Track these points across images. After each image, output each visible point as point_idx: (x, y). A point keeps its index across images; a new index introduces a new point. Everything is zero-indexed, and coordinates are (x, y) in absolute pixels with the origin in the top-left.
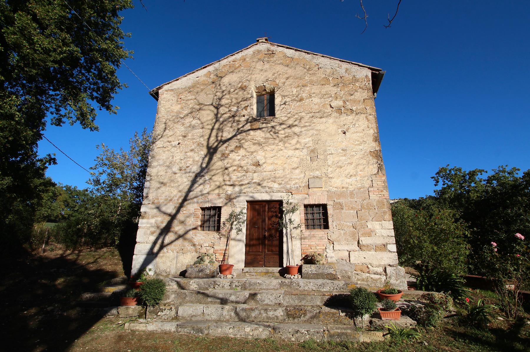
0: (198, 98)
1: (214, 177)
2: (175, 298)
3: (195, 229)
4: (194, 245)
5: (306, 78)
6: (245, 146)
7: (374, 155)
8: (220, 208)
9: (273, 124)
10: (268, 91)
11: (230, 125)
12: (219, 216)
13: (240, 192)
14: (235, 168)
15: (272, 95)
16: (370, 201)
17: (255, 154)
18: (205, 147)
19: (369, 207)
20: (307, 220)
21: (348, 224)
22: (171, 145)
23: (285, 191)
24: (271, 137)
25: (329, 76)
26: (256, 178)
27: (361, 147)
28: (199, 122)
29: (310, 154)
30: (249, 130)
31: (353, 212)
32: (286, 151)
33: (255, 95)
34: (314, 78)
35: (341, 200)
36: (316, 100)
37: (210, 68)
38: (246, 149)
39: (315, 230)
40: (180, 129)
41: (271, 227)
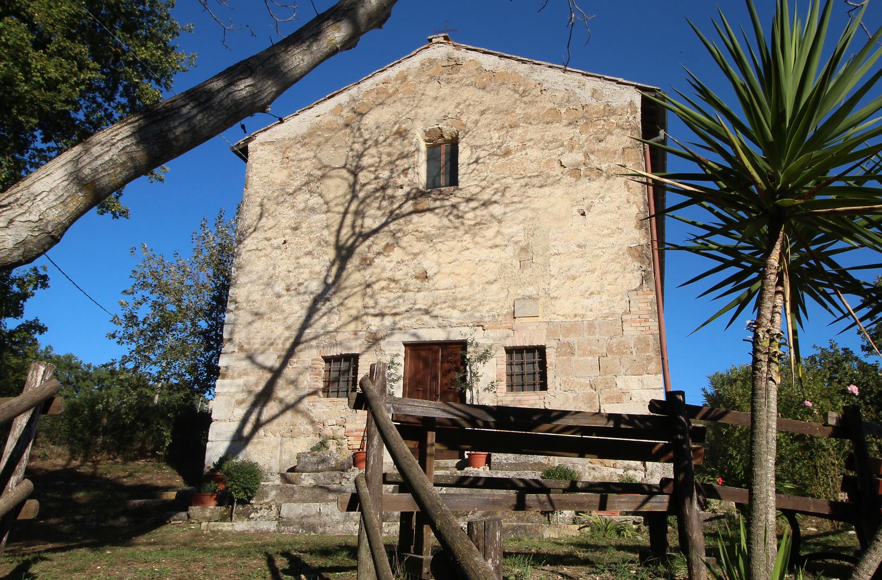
0: (319, 155)
1: (346, 301)
2: (276, 496)
3: (315, 393)
4: (312, 422)
5: (518, 111)
6: (403, 244)
7: (637, 254)
8: (356, 357)
9: (454, 200)
10: (446, 137)
11: (376, 204)
12: (356, 372)
13: (393, 329)
14: (383, 284)
15: (454, 144)
16: (623, 339)
17: (421, 256)
18: (332, 247)
19: (621, 350)
20: (510, 375)
21: (582, 380)
22: (271, 245)
23: (471, 325)
24: (450, 225)
25: (560, 105)
26: (423, 300)
27: (612, 240)
28: (321, 201)
29: (519, 254)
30: (410, 213)
31: (592, 360)
32: (474, 251)
33: (423, 146)
34: (532, 111)
35: (573, 339)
36: (534, 153)
37: (342, 98)
38: (404, 248)
39: (522, 393)
40: (286, 215)
41: (446, 388)
